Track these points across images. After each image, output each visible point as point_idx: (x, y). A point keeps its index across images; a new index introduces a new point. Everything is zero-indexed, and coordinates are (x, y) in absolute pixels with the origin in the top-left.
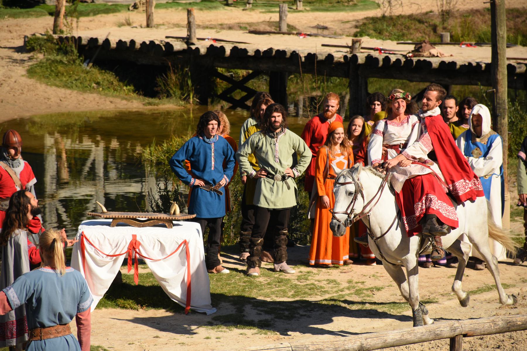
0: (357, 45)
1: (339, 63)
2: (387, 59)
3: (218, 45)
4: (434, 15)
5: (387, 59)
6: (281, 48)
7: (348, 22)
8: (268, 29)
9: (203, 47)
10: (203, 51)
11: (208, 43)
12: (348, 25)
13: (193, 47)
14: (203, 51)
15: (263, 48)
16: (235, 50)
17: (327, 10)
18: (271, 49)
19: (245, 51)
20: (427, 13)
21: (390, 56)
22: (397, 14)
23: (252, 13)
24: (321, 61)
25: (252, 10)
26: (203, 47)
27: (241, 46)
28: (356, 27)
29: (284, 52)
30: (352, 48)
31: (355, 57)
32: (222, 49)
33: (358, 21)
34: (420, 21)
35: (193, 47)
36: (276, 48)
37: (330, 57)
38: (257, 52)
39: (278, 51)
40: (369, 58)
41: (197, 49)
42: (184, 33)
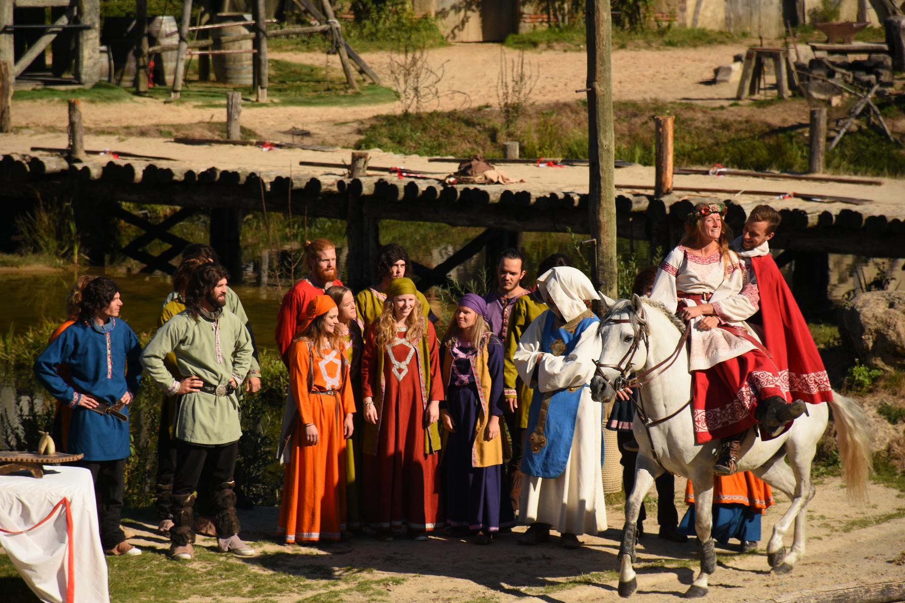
0: (361, 163)
1: (330, 194)
2: (411, 187)
3: (121, 162)
4: (492, 111)
5: (411, 187)
6: (231, 167)
7: (345, 123)
8: (208, 135)
9: (95, 165)
10: (95, 173)
11: (104, 160)
12: (346, 129)
13: (79, 166)
14: (95, 173)
15: (200, 168)
16: (150, 171)
17: (309, 103)
18: (212, 170)
19: (168, 173)
20: (480, 109)
21: (417, 182)
22: (429, 110)
23: (181, 108)
24: (299, 191)
25: (180, 102)
26: (95, 165)
27: (163, 165)
28: (359, 132)
29: (235, 175)
30: (351, 168)
31: (357, 184)
32: (129, 168)
33: (361, 122)
34: (469, 123)
35: (79, 166)
36: (221, 167)
37: (314, 183)
38: (190, 174)
39: (225, 173)
40: (381, 185)
41: (86, 170)
42: (63, 142)
